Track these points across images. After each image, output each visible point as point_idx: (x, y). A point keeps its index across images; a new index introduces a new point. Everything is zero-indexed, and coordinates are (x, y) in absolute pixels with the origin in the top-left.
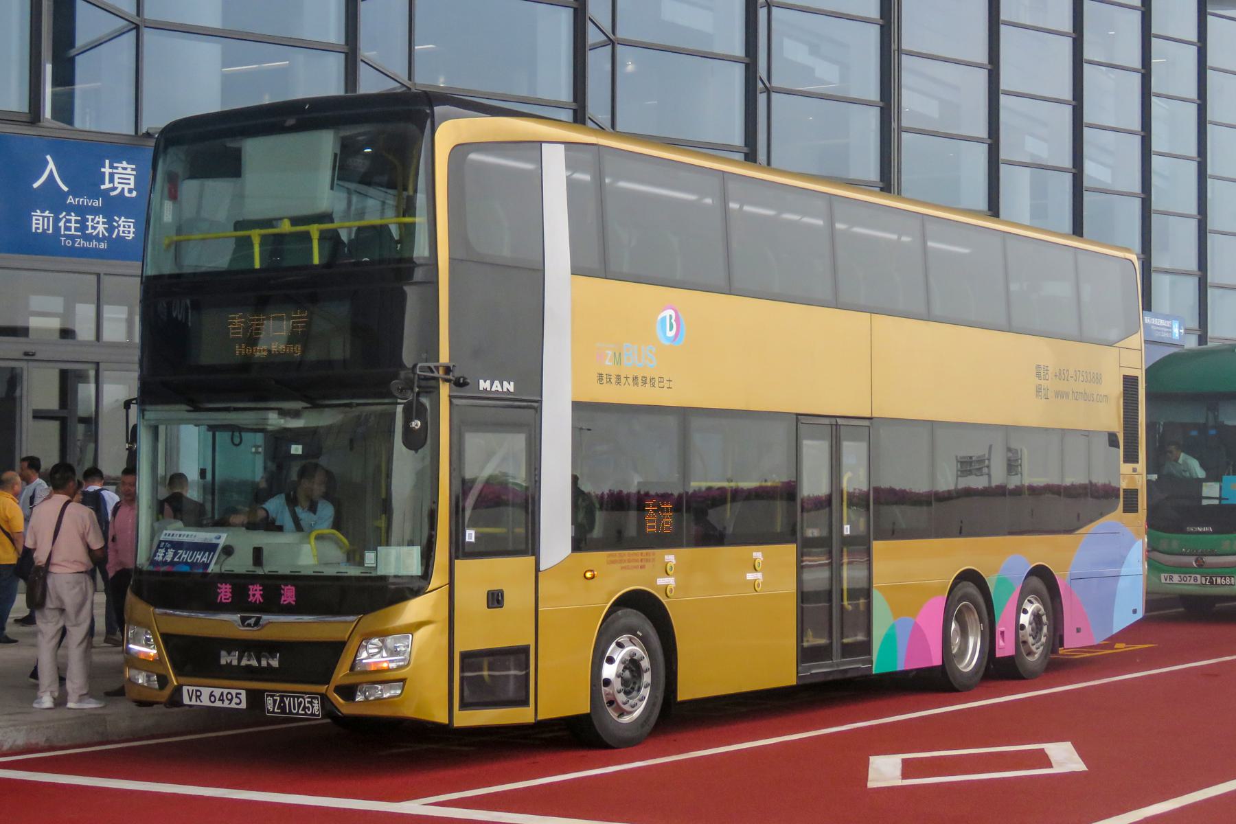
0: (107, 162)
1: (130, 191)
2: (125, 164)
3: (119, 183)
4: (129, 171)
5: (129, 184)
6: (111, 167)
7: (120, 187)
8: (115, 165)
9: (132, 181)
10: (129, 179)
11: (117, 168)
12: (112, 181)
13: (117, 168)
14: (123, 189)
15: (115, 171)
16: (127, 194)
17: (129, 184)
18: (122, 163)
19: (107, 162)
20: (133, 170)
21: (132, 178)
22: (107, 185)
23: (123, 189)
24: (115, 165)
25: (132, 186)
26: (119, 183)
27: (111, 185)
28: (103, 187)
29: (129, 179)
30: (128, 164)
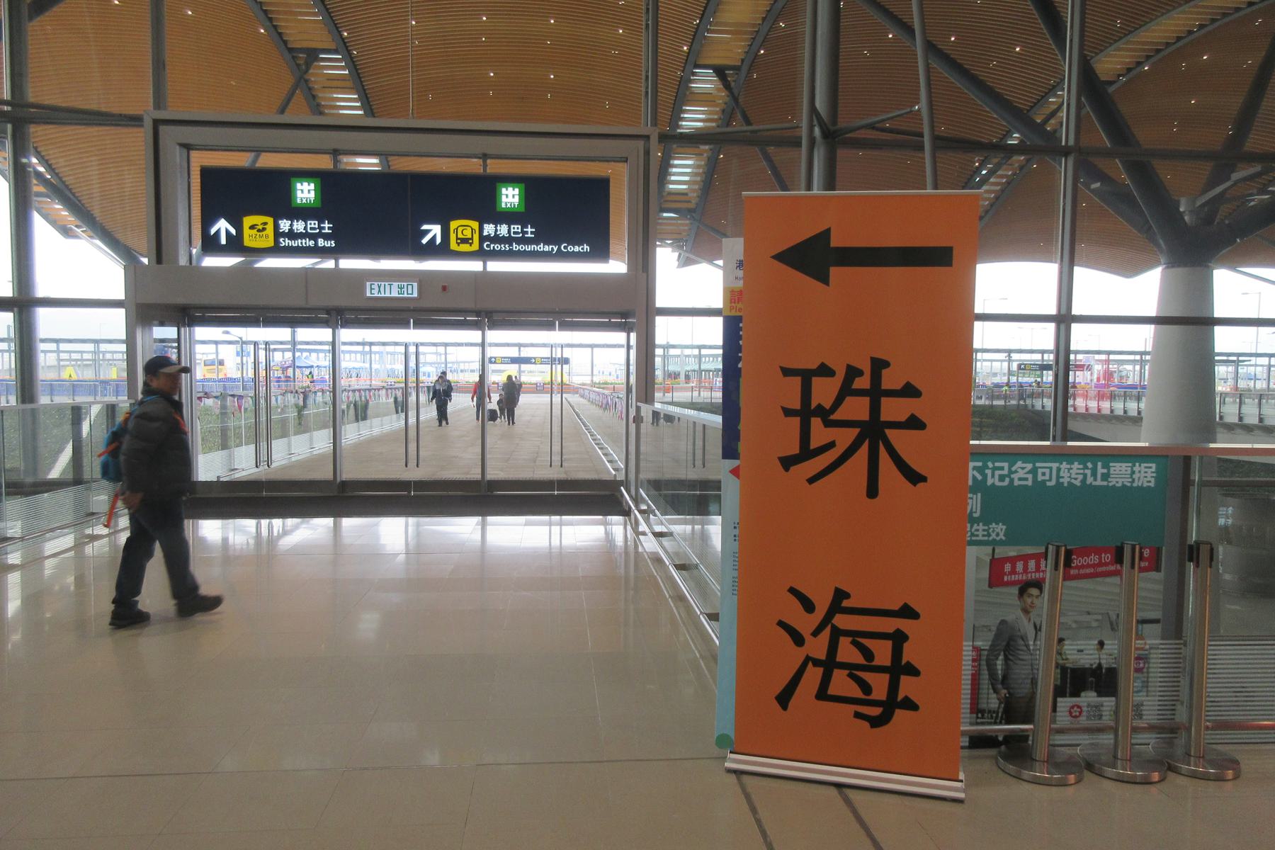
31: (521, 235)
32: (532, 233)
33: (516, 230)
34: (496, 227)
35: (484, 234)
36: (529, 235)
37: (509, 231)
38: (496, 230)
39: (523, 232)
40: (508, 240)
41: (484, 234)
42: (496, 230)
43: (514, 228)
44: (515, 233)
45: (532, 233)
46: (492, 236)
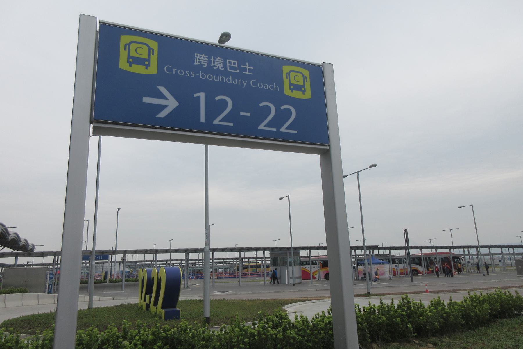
0: (212, 57)
1: (221, 68)
2: (219, 58)
3: (217, 65)
4: (220, 61)
5: (221, 65)
6: (214, 59)
7: (218, 66)
8: (216, 58)
9: (222, 64)
10: (221, 64)
11: (216, 59)
12: (214, 63)
13: (216, 59)
14: (219, 67)
15: (215, 60)
16: (220, 68)
17: (221, 65)
18: (218, 57)
19: (212, 57)
20: (222, 60)
21: (222, 63)
22: (213, 65)
23: (219, 67)
24: (216, 58)
25: (222, 66)
26: (217, 65)
27: (214, 65)
28: (211, 65)
29: (221, 64)
30: (220, 58)
31: (238, 71)
32: (250, 70)
33: (232, 65)
34: (209, 58)
35: (195, 64)
36: (247, 73)
37: (225, 65)
38: (209, 62)
39: (239, 68)
40: (225, 73)
41: (195, 64)
42: (209, 62)
43: (230, 63)
44: (231, 68)
45: (250, 70)
46: (204, 66)
